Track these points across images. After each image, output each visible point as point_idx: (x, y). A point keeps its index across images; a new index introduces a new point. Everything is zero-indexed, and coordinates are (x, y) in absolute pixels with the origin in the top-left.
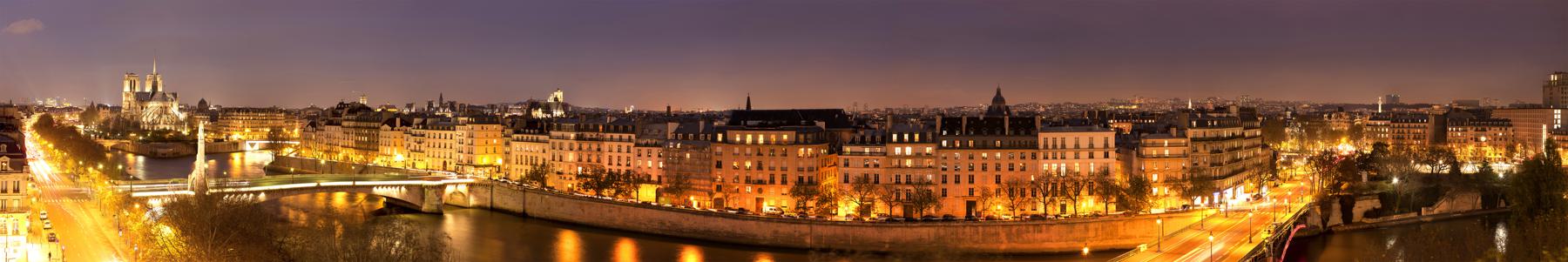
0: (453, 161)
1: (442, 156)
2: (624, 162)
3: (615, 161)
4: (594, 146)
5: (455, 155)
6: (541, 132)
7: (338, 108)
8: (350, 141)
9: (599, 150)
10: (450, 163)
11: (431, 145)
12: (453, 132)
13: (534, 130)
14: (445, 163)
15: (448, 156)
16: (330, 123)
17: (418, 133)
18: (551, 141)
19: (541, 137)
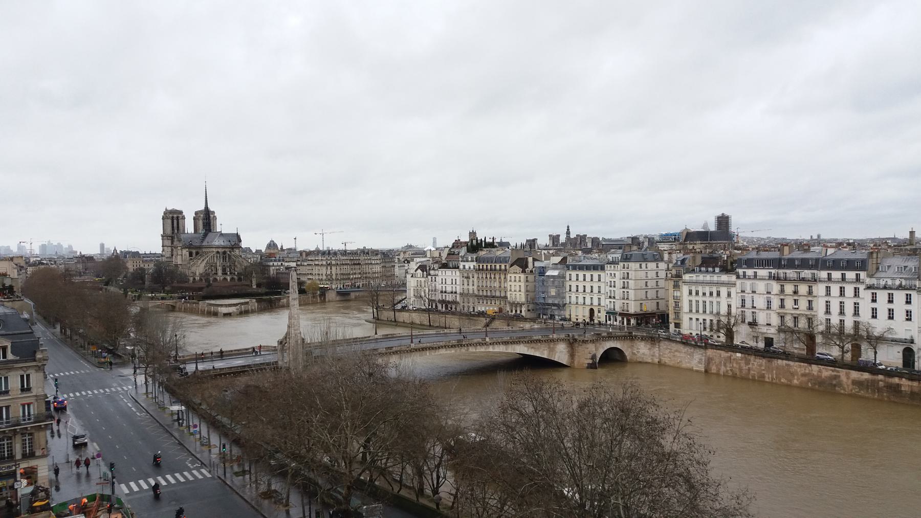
0: (602, 310)
1: (588, 302)
2: (849, 309)
3: (835, 308)
4: (803, 289)
5: (606, 302)
6: (725, 270)
7: (453, 247)
8: (471, 287)
9: (810, 293)
10: (599, 312)
12: (602, 274)
13: (714, 268)
14: (592, 311)
15: (596, 302)
16: (445, 266)
18: (739, 282)
19: (725, 278)
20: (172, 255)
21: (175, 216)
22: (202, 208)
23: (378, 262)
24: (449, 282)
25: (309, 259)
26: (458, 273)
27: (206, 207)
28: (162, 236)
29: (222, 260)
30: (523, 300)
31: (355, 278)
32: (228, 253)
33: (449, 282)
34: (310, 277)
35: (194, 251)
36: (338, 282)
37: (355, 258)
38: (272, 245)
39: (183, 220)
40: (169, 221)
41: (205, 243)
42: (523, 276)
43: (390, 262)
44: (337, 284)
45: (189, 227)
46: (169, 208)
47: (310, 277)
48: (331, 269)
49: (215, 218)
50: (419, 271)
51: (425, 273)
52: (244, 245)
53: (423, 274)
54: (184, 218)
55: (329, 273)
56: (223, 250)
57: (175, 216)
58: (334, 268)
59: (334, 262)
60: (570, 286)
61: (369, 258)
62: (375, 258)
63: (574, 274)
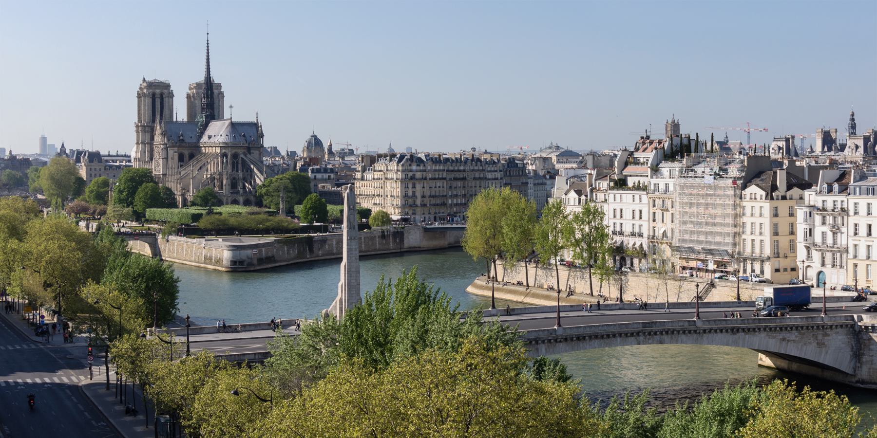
11: (863, 231)
17: (829, 205)
20: (151, 159)
21: (158, 91)
22: (201, 78)
23: (498, 175)
24: (628, 214)
25: (377, 169)
26: (645, 198)
27: (208, 78)
28: (137, 126)
29: (229, 167)
30: (767, 252)
31: (457, 204)
32: (242, 156)
33: (628, 214)
34: (377, 200)
35: (186, 153)
36: (426, 210)
37: (456, 168)
38: (315, 143)
39: (171, 100)
40: (149, 101)
41: (205, 139)
42: (767, 206)
43: (519, 175)
44: (424, 214)
45: (180, 112)
46: (150, 79)
47: (377, 200)
48: (414, 187)
49: (221, 95)
50: (573, 195)
51: (583, 197)
52: (267, 143)
53: (580, 200)
54: (171, 95)
55: (410, 194)
56: (234, 151)
57: (158, 91)
58: (419, 187)
59: (418, 175)
60: (856, 225)
61: (481, 168)
62: (493, 169)
63: (863, 202)
